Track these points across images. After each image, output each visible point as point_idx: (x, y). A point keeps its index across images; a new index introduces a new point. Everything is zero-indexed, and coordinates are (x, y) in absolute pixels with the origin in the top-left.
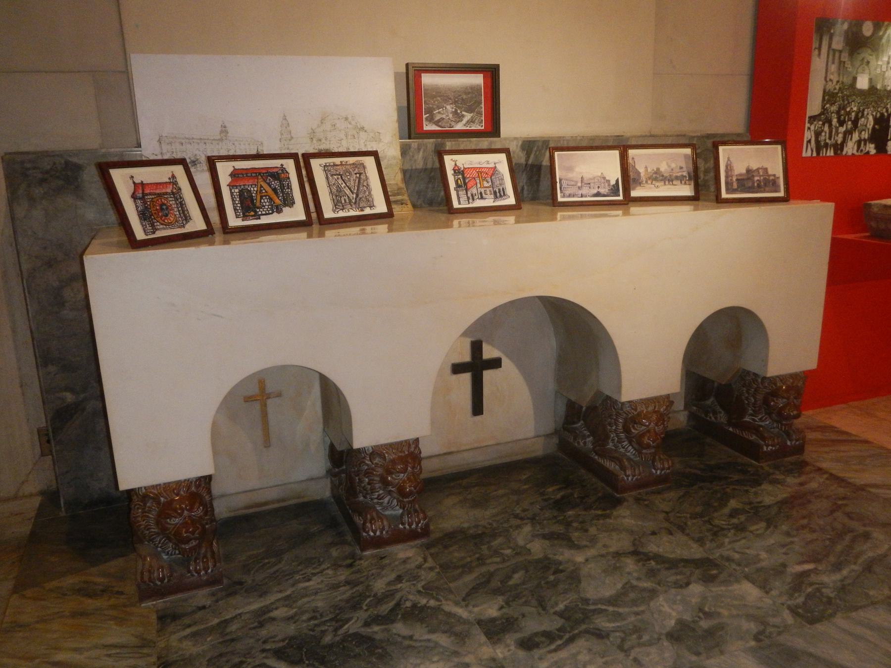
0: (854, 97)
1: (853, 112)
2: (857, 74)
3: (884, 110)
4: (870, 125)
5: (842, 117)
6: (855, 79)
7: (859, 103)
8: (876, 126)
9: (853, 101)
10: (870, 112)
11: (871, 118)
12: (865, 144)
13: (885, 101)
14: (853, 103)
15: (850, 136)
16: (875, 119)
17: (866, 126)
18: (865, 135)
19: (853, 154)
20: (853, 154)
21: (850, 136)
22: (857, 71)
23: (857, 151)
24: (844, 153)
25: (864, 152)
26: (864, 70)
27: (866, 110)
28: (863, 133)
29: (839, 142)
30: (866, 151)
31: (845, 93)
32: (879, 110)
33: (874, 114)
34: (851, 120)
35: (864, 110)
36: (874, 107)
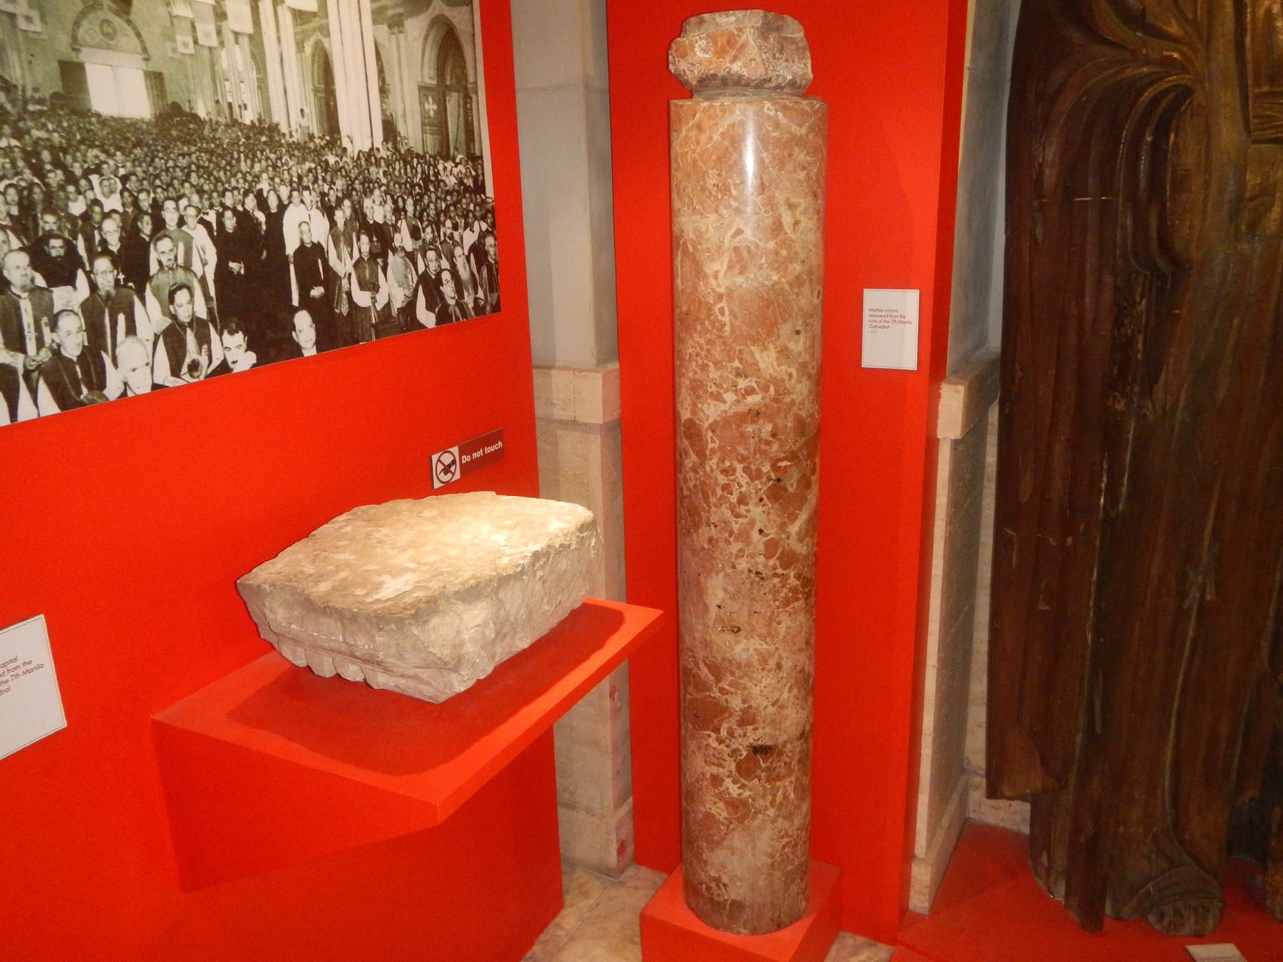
0: (96, 152)
1: (106, 216)
2: (77, 50)
3: (251, 202)
4: (204, 264)
5: (56, 243)
6: (72, 73)
7: (124, 179)
8: (234, 266)
9: (98, 170)
10: (192, 211)
11: (201, 238)
12: (203, 340)
13: (244, 167)
14: (95, 178)
15: (121, 318)
16: (220, 238)
17: (187, 267)
18: (193, 306)
19: (155, 387)
20: (155, 387)
21: (121, 318)
22: (75, 39)
23: (175, 372)
24: (112, 391)
25: (204, 371)
26: (111, 36)
27: (169, 205)
28: (182, 296)
29: (72, 350)
30: (216, 363)
31: (36, 133)
32: (229, 201)
33: (211, 217)
34: (106, 252)
35: (157, 207)
36: (200, 192)
